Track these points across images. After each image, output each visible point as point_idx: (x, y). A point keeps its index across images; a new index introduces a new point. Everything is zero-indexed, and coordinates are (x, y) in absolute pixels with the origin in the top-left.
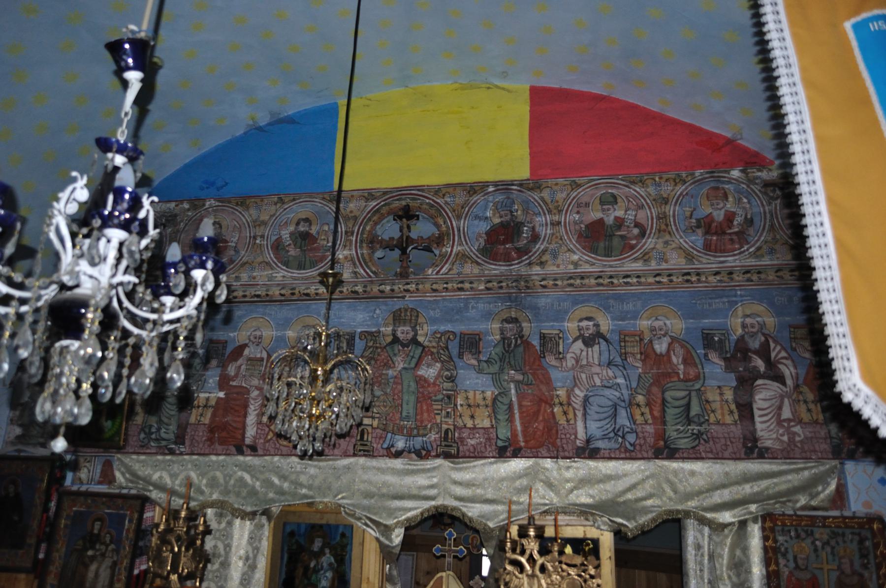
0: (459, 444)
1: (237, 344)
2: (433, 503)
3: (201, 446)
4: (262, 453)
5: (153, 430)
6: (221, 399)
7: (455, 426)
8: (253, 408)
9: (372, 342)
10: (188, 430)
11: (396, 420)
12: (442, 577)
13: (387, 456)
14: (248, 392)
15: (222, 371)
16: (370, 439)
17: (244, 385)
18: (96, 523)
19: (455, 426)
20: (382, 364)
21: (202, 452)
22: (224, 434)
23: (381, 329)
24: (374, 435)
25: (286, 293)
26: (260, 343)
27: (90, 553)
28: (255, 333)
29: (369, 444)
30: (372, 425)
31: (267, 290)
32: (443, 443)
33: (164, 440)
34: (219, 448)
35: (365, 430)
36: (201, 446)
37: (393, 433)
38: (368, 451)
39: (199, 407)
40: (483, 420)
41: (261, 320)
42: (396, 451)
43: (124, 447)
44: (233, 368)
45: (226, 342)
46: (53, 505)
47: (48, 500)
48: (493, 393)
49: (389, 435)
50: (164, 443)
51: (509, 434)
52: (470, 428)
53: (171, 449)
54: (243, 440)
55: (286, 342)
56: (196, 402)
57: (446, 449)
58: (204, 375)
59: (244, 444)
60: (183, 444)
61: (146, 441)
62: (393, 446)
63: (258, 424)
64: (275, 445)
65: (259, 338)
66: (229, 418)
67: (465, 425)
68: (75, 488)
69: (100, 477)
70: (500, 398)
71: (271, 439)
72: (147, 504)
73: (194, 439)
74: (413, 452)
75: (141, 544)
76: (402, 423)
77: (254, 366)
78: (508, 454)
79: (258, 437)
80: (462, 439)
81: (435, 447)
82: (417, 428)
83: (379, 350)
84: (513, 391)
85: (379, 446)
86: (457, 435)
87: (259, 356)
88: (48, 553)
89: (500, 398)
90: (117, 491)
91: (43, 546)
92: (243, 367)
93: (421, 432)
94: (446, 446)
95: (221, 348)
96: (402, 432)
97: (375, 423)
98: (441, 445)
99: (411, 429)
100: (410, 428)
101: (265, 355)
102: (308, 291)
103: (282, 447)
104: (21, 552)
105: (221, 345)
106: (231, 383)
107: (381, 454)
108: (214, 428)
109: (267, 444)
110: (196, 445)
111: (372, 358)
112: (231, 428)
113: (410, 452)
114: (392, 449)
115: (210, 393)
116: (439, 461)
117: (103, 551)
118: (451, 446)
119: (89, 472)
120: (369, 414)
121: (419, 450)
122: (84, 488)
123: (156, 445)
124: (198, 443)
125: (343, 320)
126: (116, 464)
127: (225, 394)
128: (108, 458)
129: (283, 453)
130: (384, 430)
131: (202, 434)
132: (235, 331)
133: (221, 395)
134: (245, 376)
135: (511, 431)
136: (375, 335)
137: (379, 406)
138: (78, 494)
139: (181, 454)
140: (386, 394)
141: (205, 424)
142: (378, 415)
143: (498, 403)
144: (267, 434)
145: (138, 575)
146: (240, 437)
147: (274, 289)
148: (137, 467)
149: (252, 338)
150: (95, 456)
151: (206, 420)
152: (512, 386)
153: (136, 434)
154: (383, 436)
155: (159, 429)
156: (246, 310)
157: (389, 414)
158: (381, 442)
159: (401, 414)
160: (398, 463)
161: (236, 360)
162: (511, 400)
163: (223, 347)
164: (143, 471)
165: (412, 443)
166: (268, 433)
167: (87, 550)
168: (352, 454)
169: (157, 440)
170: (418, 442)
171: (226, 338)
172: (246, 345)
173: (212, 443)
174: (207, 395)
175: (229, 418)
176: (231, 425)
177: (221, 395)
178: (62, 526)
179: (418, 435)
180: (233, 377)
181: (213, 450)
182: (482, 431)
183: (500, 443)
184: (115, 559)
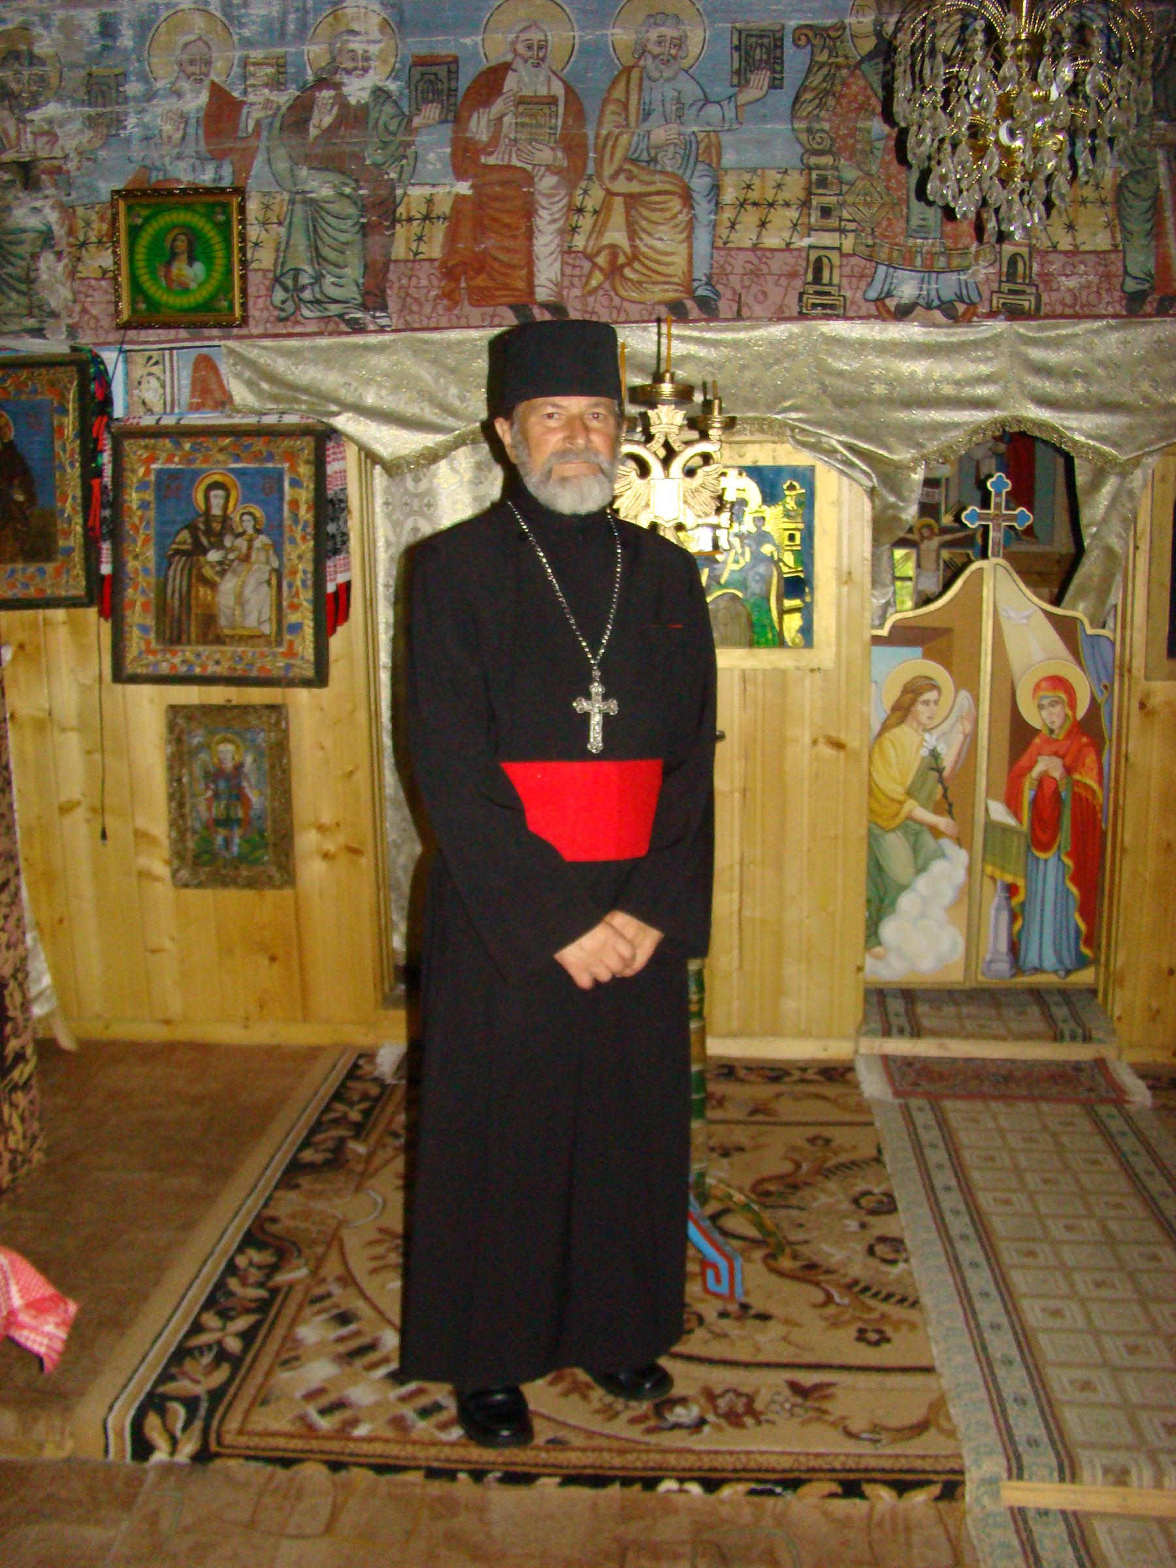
0: (1041, 286)
1: (485, 65)
2: (997, 414)
3: (427, 310)
5: (305, 280)
6: (464, 197)
7: (1031, 247)
8: (548, 218)
9: (826, 52)
10: (392, 276)
11: (896, 236)
12: (981, 569)
13: (876, 317)
14: (529, 179)
15: (455, 132)
16: (836, 280)
17: (515, 162)
18: (213, 493)
19: (1031, 247)
20: (854, 106)
21: (433, 324)
22: (480, 281)
23: (847, 21)
24: (847, 270)
26: (543, 59)
27: (214, 556)
28: (524, 36)
29: (834, 290)
30: (839, 249)
32: (1006, 287)
33: (335, 301)
34: (475, 313)
35: (825, 260)
36: (427, 310)
37: (889, 266)
38: (832, 307)
39: (410, 220)
40: (1094, 234)
42: (898, 306)
43: (245, 321)
44: (483, 123)
45: (456, 60)
46: (106, 458)
47: (90, 453)
48: (1116, 174)
49: (882, 270)
50: (334, 309)
51: (1151, 265)
52: (1065, 253)
53: (356, 321)
54: (532, 293)
56: (401, 210)
57: (1012, 300)
58: (409, 144)
59: (535, 303)
60: (384, 308)
61: (290, 307)
62: (889, 294)
63: (563, 253)
64: (611, 300)
65: (540, 48)
66: (490, 243)
67: (1055, 247)
68: (148, 421)
69: (193, 396)
70: (1131, 184)
71: (599, 287)
72: (330, 444)
73: (408, 295)
74: (938, 307)
75: (331, 528)
76: (910, 242)
77: (532, 116)
78: (1148, 309)
79: (566, 283)
80: (1047, 277)
81: (986, 295)
82: (947, 253)
83: (844, 72)
84: (1162, 169)
85: (859, 294)
86: (1036, 268)
87: (543, 91)
88: (118, 562)
89: (1131, 184)
90: (252, 420)
91: (106, 547)
92: (508, 120)
93: (955, 262)
94: (1011, 292)
95: (442, 71)
96: (912, 264)
97: (848, 244)
98: (999, 292)
99: (932, 255)
100: (928, 252)
101: (558, 89)
103: (626, 305)
104: (50, 567)
105: (445, 68)
106: (483, 160)
107: (862, 313)
108: (454, 267)
109: (591, 300)
110: (415, 308)
111: (827, 92)
113: (929, 307)
114: (888, 302)
115: (434, 186)
116: (999, 326)
117: (244, 550)
118: (1023, 292)
119: (163, 386)
120: (833, 222)
121: (951, 302)
122: (168, 421)
123: (319, 314)
124: (421, 305)
126: (225, 368)
127: (472, 187)
128: (205, 351)
130: (870, 259)
131: (426, 281)
133: (464, 188)
134: (515, 141)
135: (1157, 255)
136: (833, 34)
137: (854, 205)
138: (157, 433)
139: (382, 330)
140: (868, 175)
141: (432, 260)
142: (853, 226)
143: (1127, 194)
144: (589, 277)
145: (336, 594)
146: (521, 285)
148: (281, 366)
149: (521, 48)
150: (171, 349)
151: (435, 248)
152: (1160, 155)
153: (263, 292)
154: (868, 272)
155: (318, 278)
157: (879, 224)
158: (863, 285)
159: (908, 220)
160: (895, 332)
161: (487, 103)
162: (1158, 190)
163: (449, 72)
164: (307, 374)
165: (934, 286)
166: (591, 272)
167: (205, 552)
168: (795, 314)
169: (317, 302)
170: (948, 285)
171: (454, 51)
172: (505, 67)
173: (456, 303)
174: (427, 191)
175: (490, 243)
176: (495, 259)
177: (464, 188)
178: (134, 506)
179: (949, 269)
180: (488, 145)
181: (458, 318)
182: (1091, 259)
183: (1131, 286)
184: (276, 564)
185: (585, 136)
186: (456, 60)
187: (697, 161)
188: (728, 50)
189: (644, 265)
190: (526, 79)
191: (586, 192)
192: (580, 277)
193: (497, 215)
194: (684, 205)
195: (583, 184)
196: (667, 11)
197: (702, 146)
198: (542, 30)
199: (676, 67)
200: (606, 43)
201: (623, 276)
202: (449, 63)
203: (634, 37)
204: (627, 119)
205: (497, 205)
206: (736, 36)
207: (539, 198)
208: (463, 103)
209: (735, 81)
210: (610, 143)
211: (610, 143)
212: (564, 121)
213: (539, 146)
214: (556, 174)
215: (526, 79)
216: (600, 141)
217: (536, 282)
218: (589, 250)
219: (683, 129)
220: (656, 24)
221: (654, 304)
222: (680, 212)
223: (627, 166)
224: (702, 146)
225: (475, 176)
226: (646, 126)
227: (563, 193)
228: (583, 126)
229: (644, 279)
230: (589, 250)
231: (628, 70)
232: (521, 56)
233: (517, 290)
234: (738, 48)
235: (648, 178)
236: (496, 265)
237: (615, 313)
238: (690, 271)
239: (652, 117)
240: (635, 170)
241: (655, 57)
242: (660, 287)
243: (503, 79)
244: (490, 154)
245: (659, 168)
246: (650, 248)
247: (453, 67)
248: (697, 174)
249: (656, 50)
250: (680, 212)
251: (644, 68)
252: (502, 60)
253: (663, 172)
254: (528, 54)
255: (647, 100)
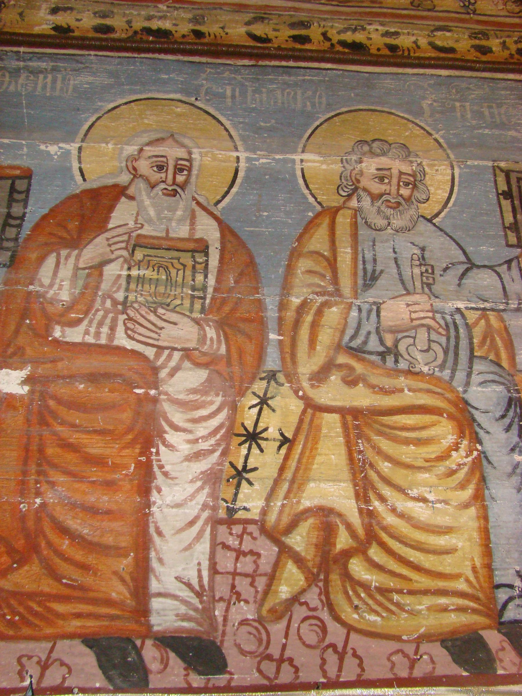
4: (254, 678)
8: (185, 449)
25: (272, 34)
26: (183, 186)
31: (195, 20)
41: (180, 109)
45: (28, 175)
55: (295, 189)
64: (324, 629)
65: (178, 169)
102: (359, 37)
106: (57, 333)
112: (65, 544)
125: (512, 133)
127: (27, 381)
129: (370, 674)
132: (69, 138)
147: (225, 17)
156: (111, 74)
166: (277, 565)
171: (25, 162)
180: (70, 307)
185: (260, 304)
186: (28, 175)
187: (472, 357)
188: (493, 196)
189: (390, 552)
190: (152, 212)
191: (264, 401)
192: (252, 577)
193: (75, 437)
194: (461, 435)
195: (259, 387)
196: (391, 139)
197: (478, 332)
198: (183, 146)
199: (412, 212)
200: (294, 175)
201: (347, 576)
202: (14, 179)
203: (337, 167)
204: (335, 280)
205: (77, 418)
206: (501, 179)
207: (166, 407)
208: (28, 239)
209: (513, 239)
210: (309, 319)
211: (309, 319)
212: (218, 281)
213: (173, 317)
214: (205, 365)
215: (152, 212)
216: (290, 315)
217: (154, 586)
218: (272, 518)
219: (438, 304)
220: (372, 154)
221: (419, 640)
222: (456, 447)
223: (342, 359)
224: (478, 332)
225: (36, 362)
226: (371, 296)
227: (219, 400)
228: (256, 290)
229: (391, 583)
230: (272, 518)
231: (334, 212)
232: (147, 180)
233: (109, 602)
234: (508, 195)
235: (387, 382)
236: (65, 544)
237: (332, 658)
238: (489, 567)
239: (381, 282)
240: (359, 368)
241: (375, 198)
242: (427, 601)
243: (111, 208)
244: (78, 322)
245: (403, 365)
246: (402, 516)
247: (20, 185)
248: (475, 379)
249: (376, 188)
250: (456, 447)
251: (357, 211)
252: (110, 181)
253: (409, 373)
254: (156, 176)
255: (369, 256)
